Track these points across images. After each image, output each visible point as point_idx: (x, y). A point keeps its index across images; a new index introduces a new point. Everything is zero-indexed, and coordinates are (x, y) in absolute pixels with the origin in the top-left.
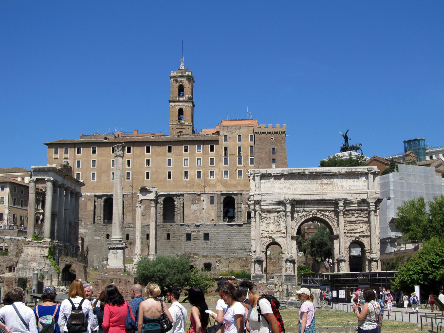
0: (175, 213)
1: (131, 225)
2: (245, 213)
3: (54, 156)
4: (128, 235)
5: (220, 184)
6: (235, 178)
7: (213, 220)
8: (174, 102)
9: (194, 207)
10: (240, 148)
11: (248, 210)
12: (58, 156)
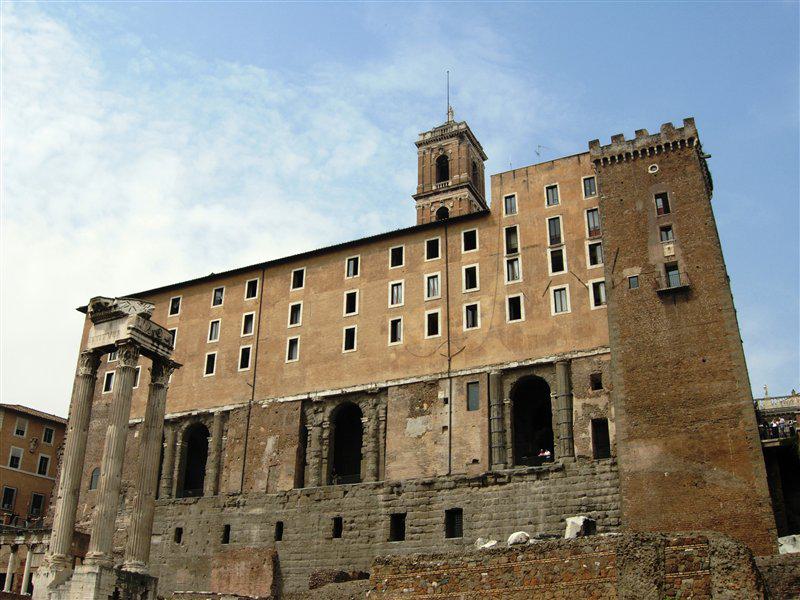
0: (363, 451)
1: (240, 499)
2: (585, 425)
4: (227, 528)
5: (496, 341)
6: (545, 316)
7: (475, 461)
8: (427, 196)
9: (416, 426)
10: (554, 221)
11: (593, 415)
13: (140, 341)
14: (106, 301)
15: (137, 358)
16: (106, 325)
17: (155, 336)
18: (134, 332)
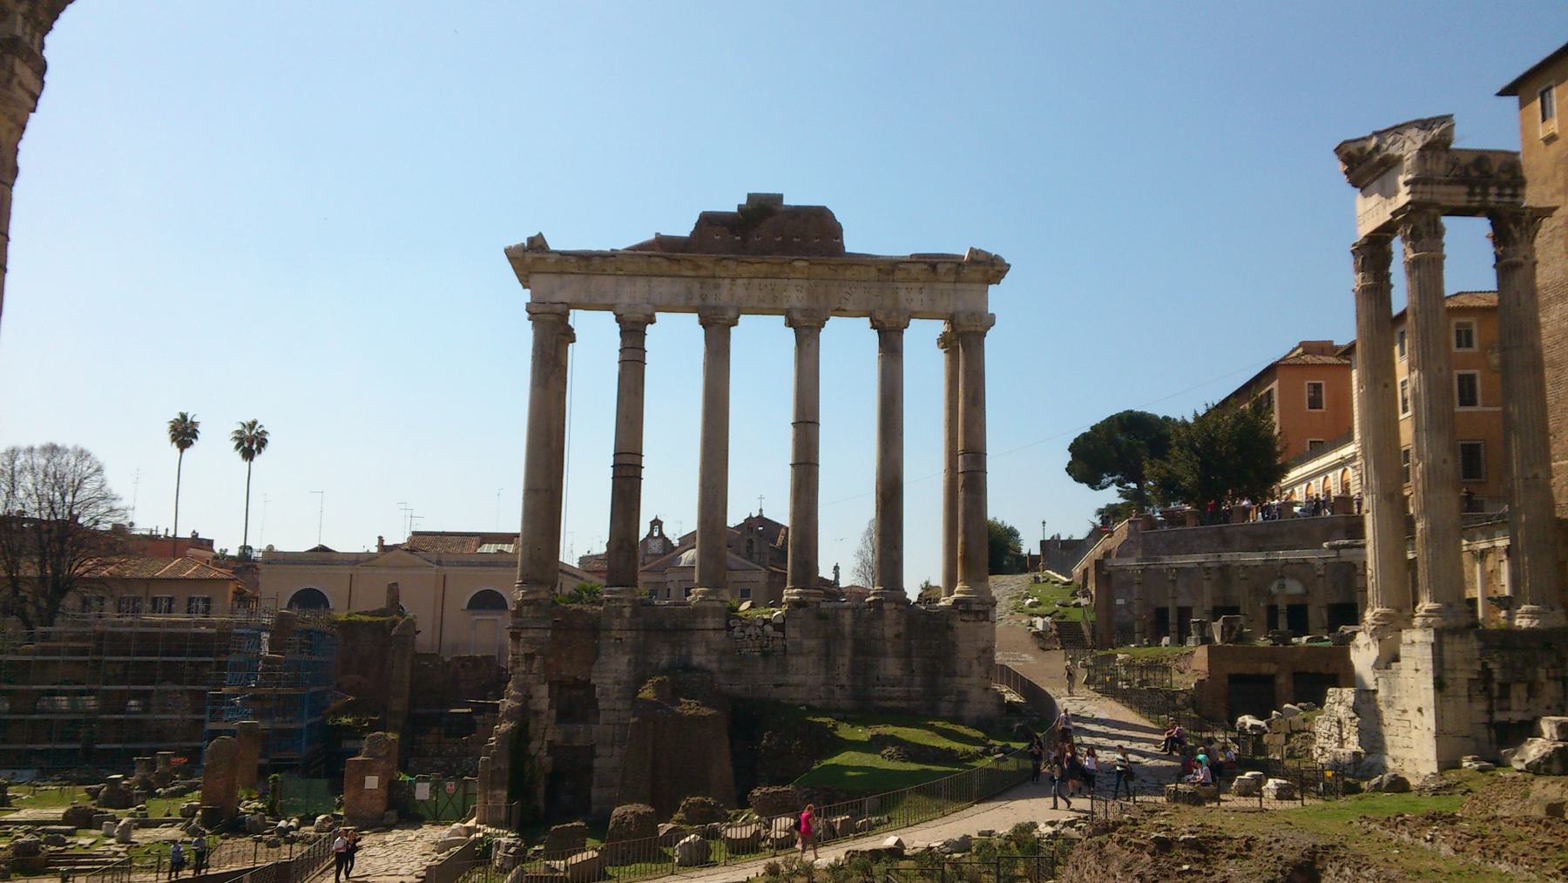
3: (1542, 132)
12: (1553, 126)
13: (1437, 197)
14: (1359, 145)
15: (1438, 232)
16: (1375, 185)
17: (1474, 174)
18: (1419, 188)
